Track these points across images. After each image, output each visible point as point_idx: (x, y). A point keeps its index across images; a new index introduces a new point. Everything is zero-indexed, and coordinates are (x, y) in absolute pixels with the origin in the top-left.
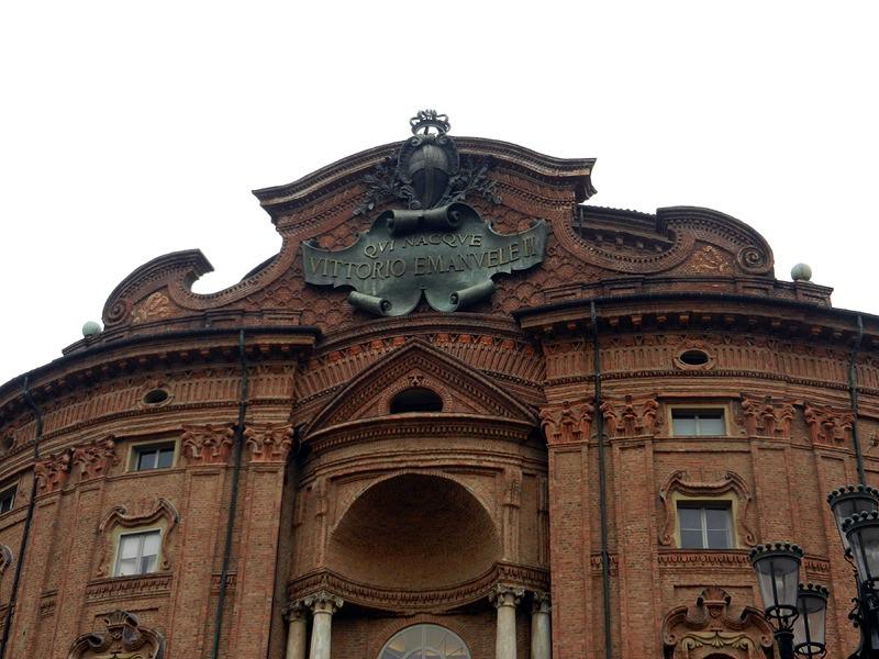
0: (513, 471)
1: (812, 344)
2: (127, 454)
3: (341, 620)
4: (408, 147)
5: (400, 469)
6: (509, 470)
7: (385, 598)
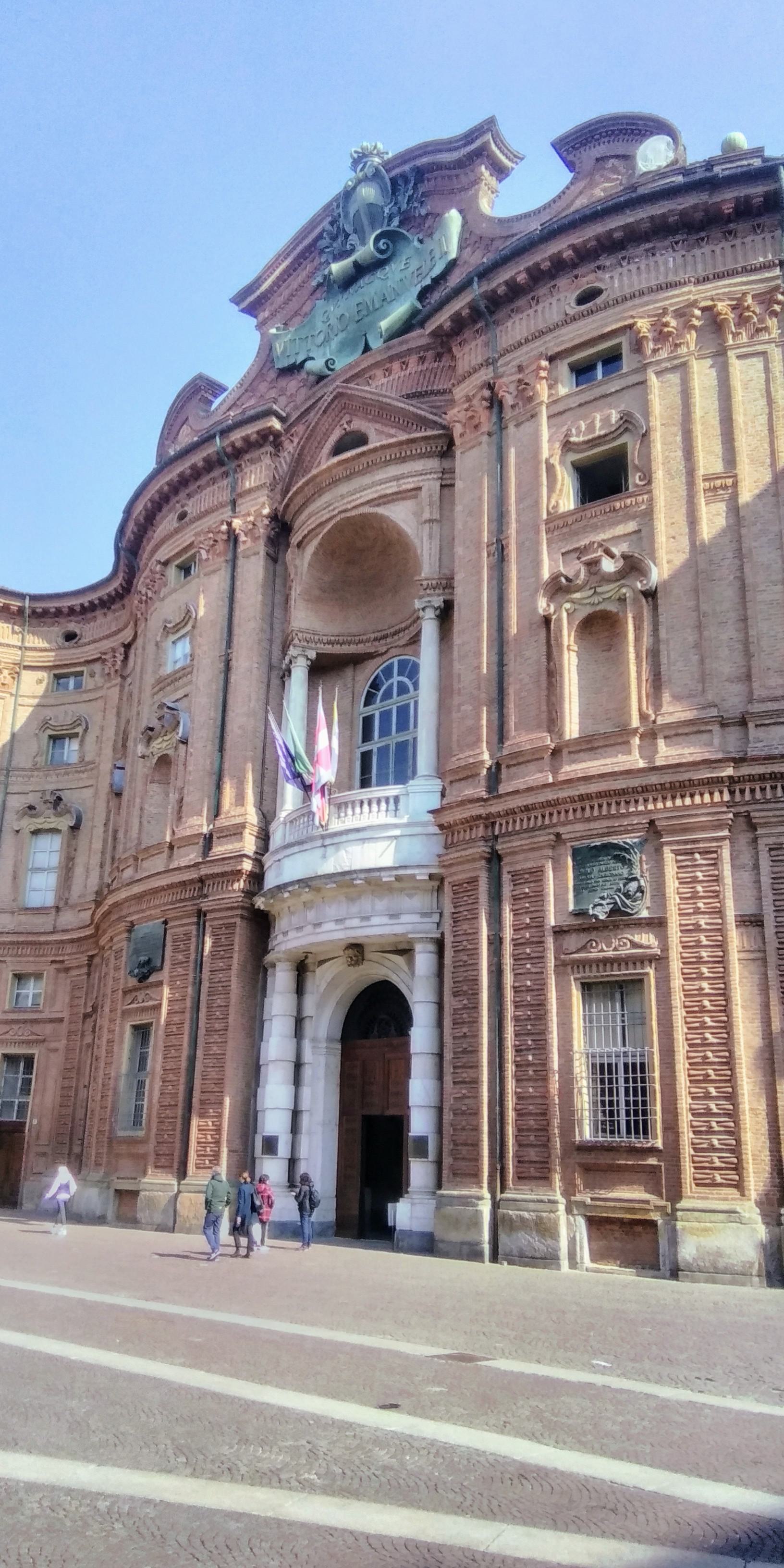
0: (431, 486)
1: (732, 226)
2: (172, 571)
4: (347, 194)
5: (335, 516)
6: (426, 486)
7: (360, 642)
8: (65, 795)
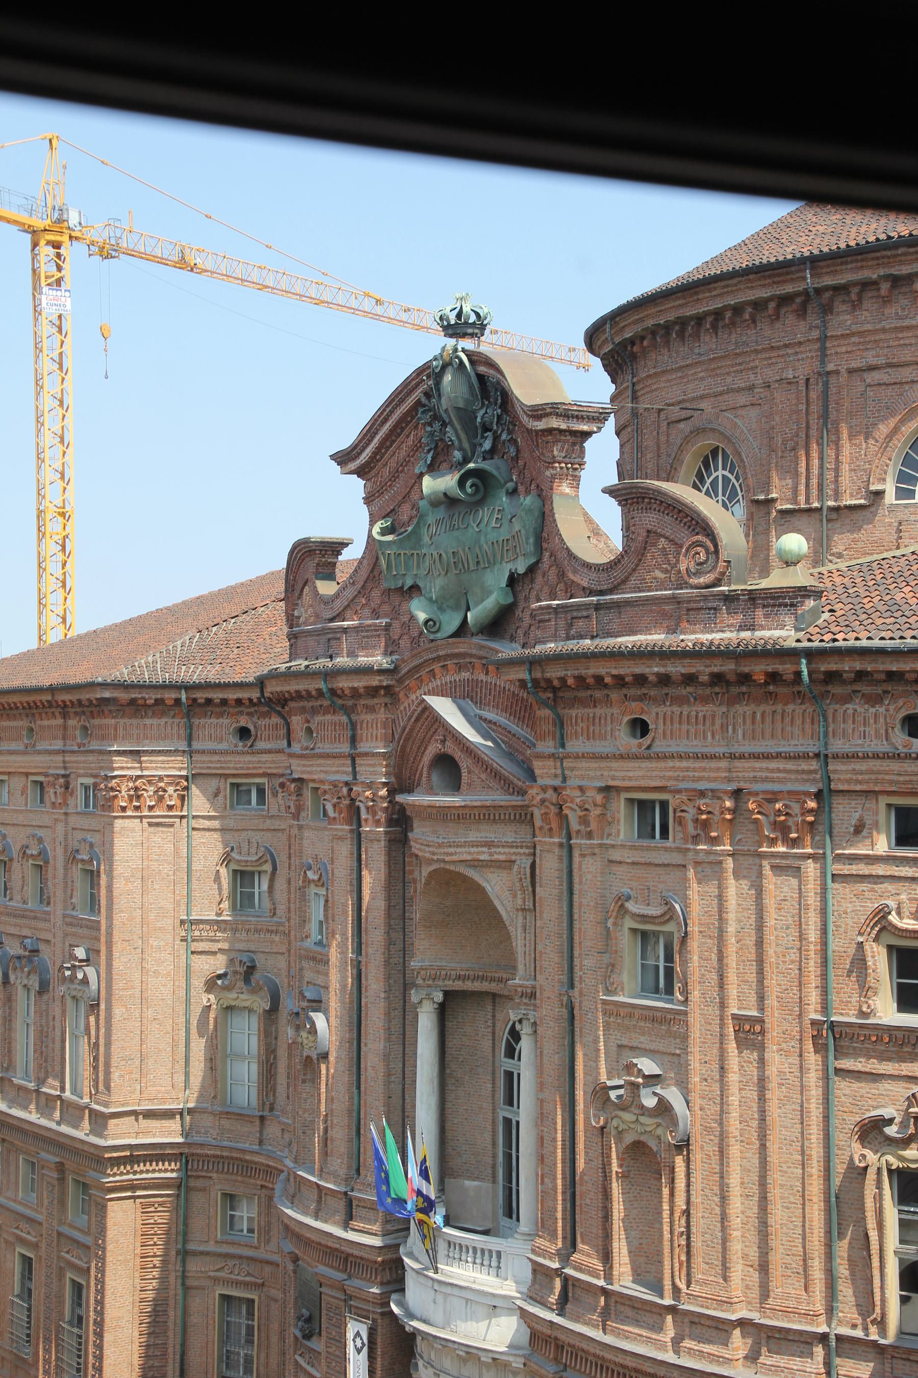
3: (443, 1012)
8: (260, 961)
